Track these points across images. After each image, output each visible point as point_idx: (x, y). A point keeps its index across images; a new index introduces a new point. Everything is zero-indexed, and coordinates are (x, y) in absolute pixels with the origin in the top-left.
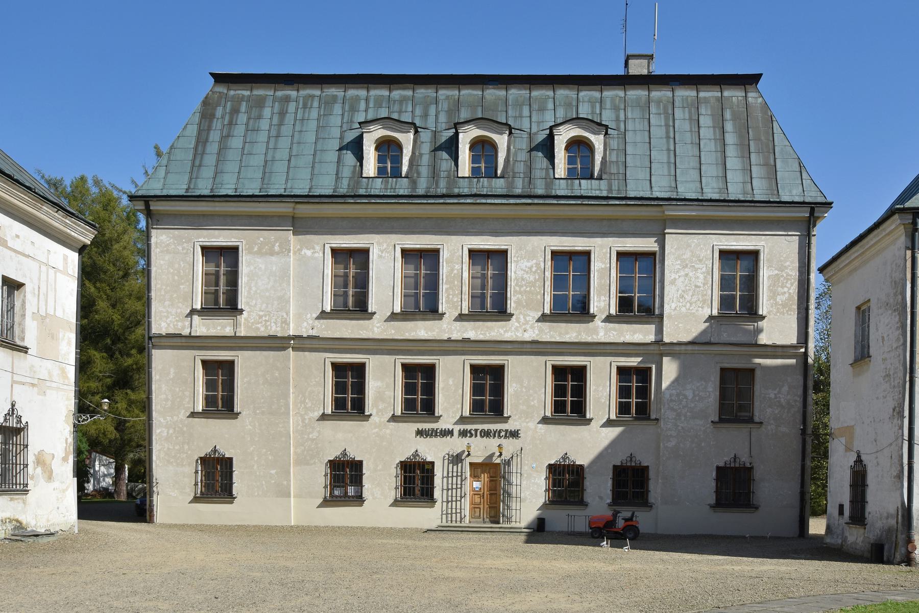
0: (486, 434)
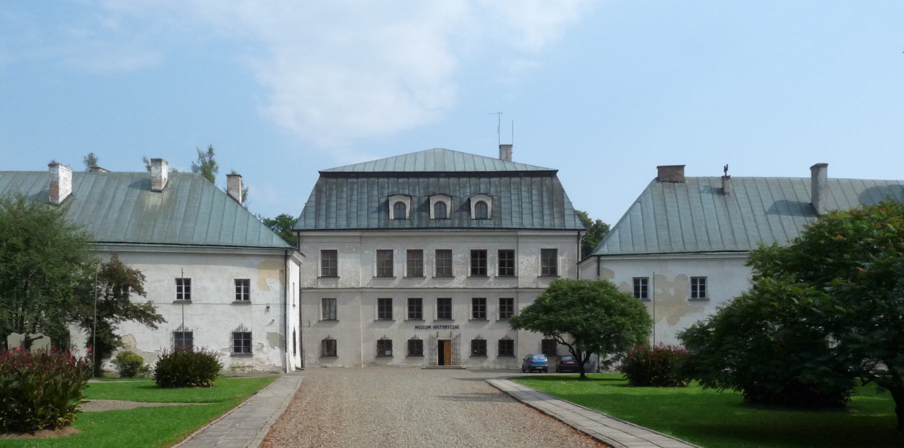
0: (445, 327)
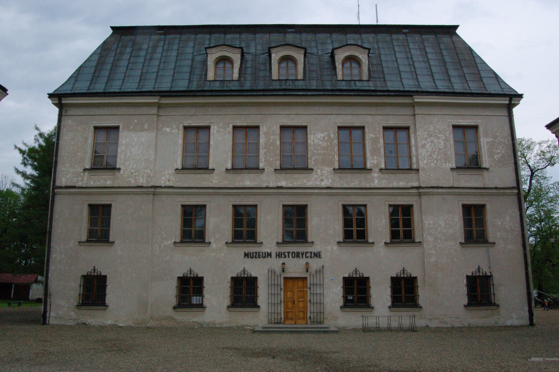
0: (297, 255)
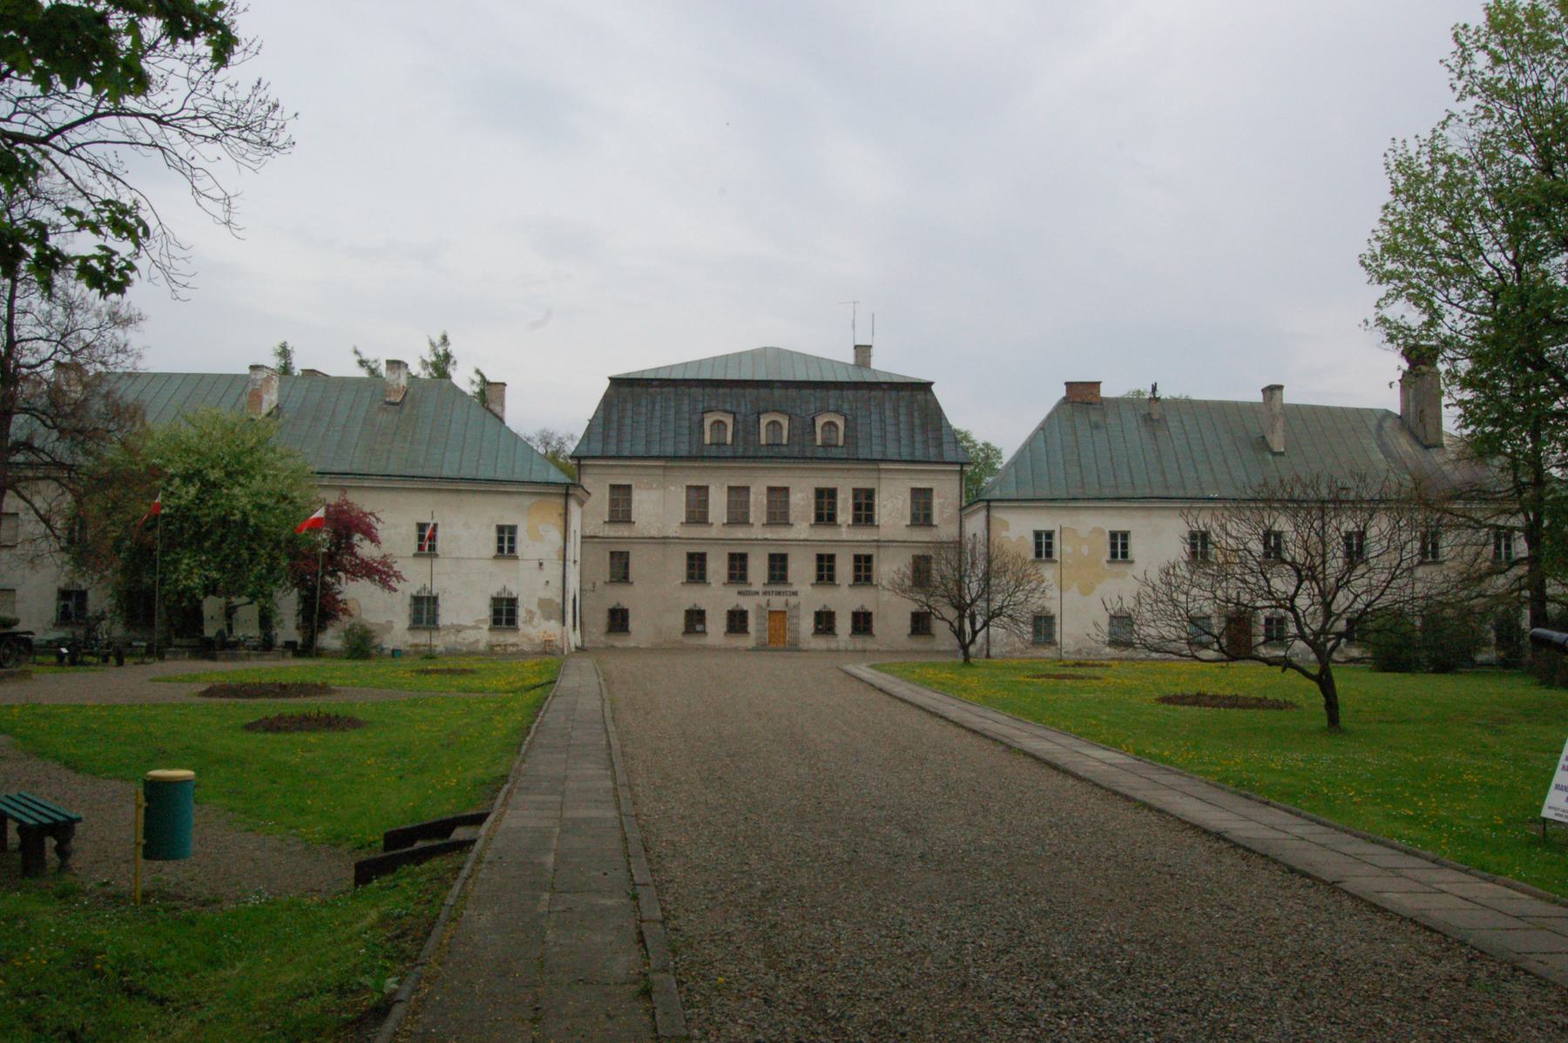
0: (779, 593)
